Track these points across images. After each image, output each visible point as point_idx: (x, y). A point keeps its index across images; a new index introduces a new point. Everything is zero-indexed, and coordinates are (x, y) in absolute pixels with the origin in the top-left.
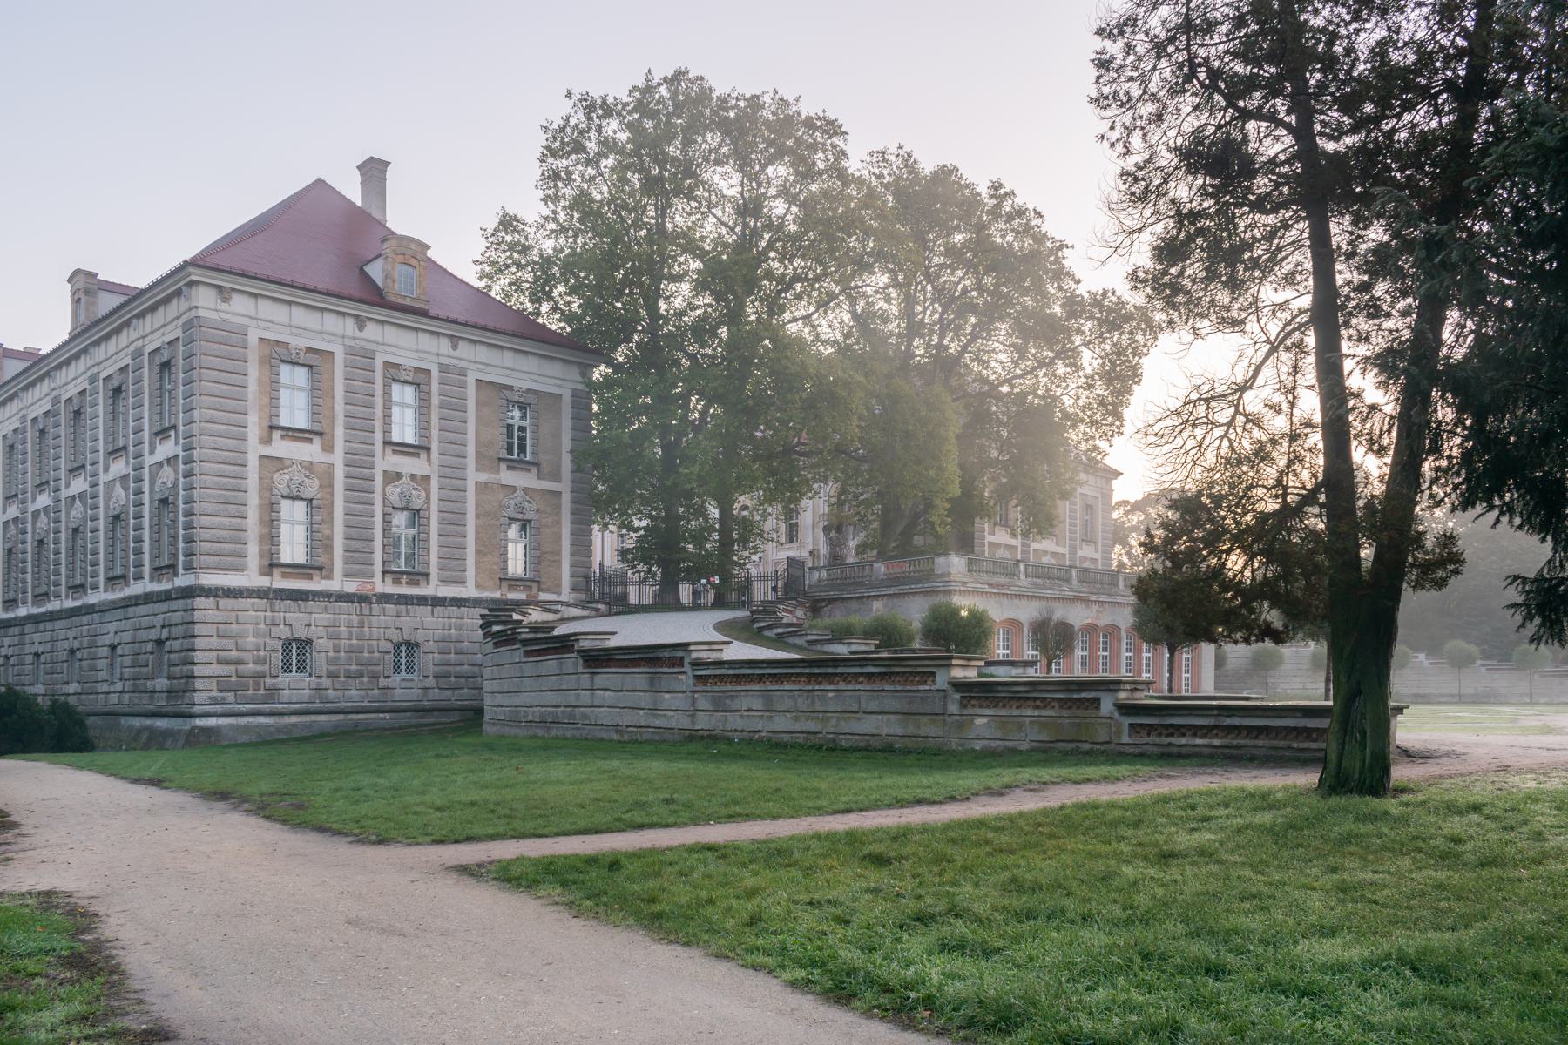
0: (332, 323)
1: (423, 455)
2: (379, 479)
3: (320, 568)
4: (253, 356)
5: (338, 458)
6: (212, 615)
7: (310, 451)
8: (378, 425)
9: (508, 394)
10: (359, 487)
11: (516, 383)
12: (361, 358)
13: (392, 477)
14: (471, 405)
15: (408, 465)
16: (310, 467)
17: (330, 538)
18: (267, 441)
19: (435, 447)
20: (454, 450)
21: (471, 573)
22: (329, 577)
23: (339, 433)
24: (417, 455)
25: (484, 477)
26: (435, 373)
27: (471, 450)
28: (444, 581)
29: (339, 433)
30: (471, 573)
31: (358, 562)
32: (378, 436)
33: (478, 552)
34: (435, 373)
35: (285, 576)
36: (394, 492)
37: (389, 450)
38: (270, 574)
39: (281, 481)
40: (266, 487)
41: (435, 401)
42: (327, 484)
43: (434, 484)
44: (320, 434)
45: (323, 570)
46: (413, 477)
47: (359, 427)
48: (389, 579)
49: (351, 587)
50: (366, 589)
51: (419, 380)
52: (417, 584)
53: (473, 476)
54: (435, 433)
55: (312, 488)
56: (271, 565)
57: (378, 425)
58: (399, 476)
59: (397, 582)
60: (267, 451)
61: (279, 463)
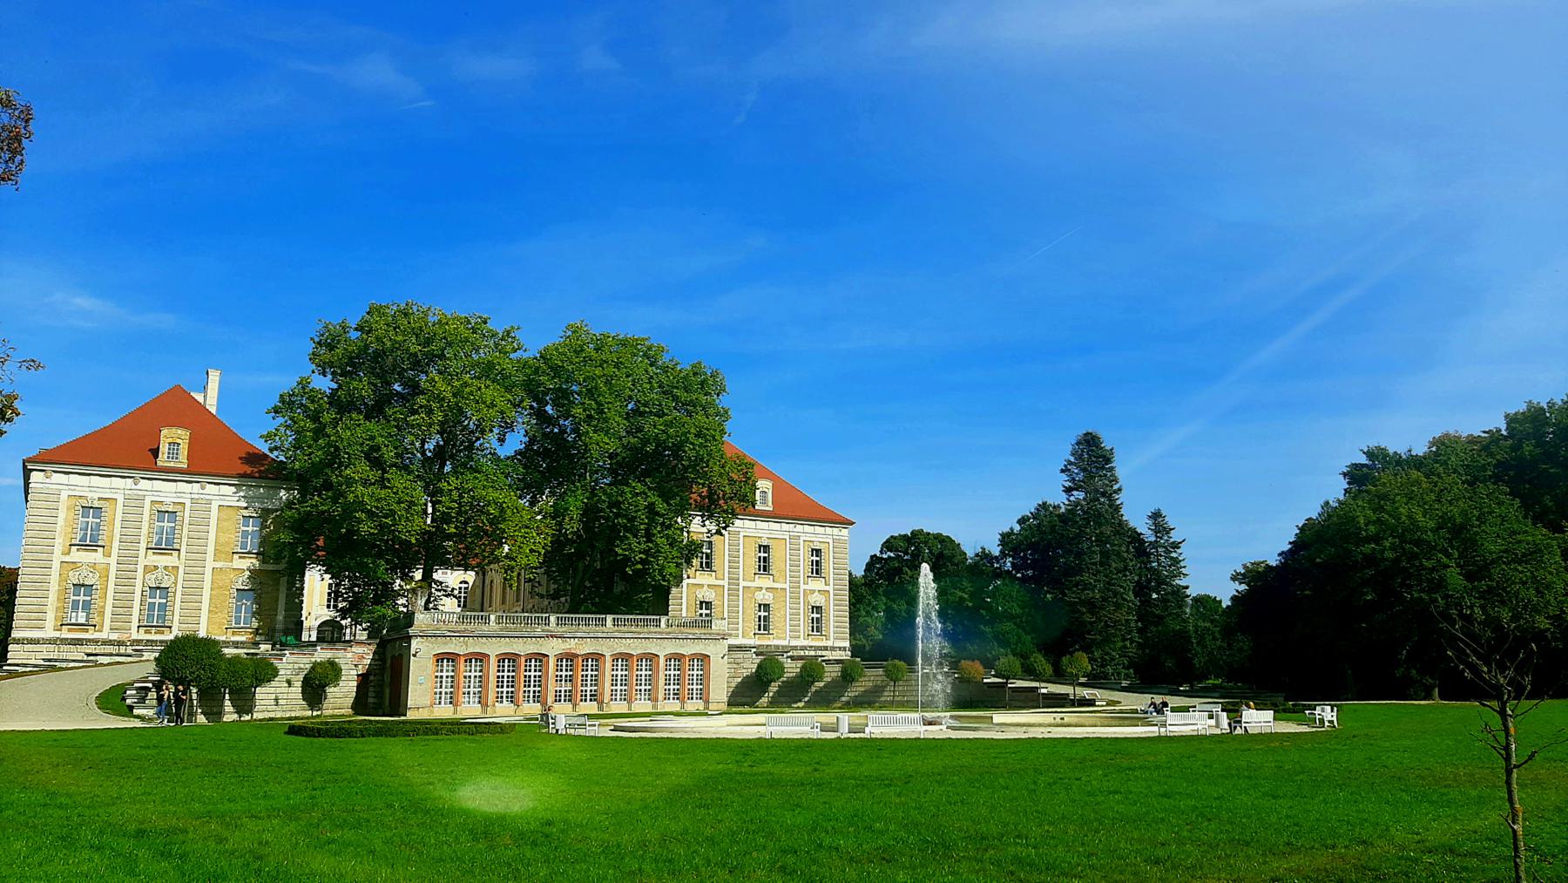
0: (117, 482)
1: (175, 554)
2: (140, 570)
4: (63, 507)
5: (113, 560)
6: (18, 655)
7: (97, 557)
10: (125, 579)
12: (135, 502)
14: (213, 522)
15: (162, 561)
23: (116, 544)
25: (219, 565)
27: (211, 549)
29: (116, 544)
32: (143, 545)
43: (181, 571)
46: (166, 568)
49: (114, 636)
50: (124, 637)
53: (210, 564)
58: (156, 567)
60: (67, 559)
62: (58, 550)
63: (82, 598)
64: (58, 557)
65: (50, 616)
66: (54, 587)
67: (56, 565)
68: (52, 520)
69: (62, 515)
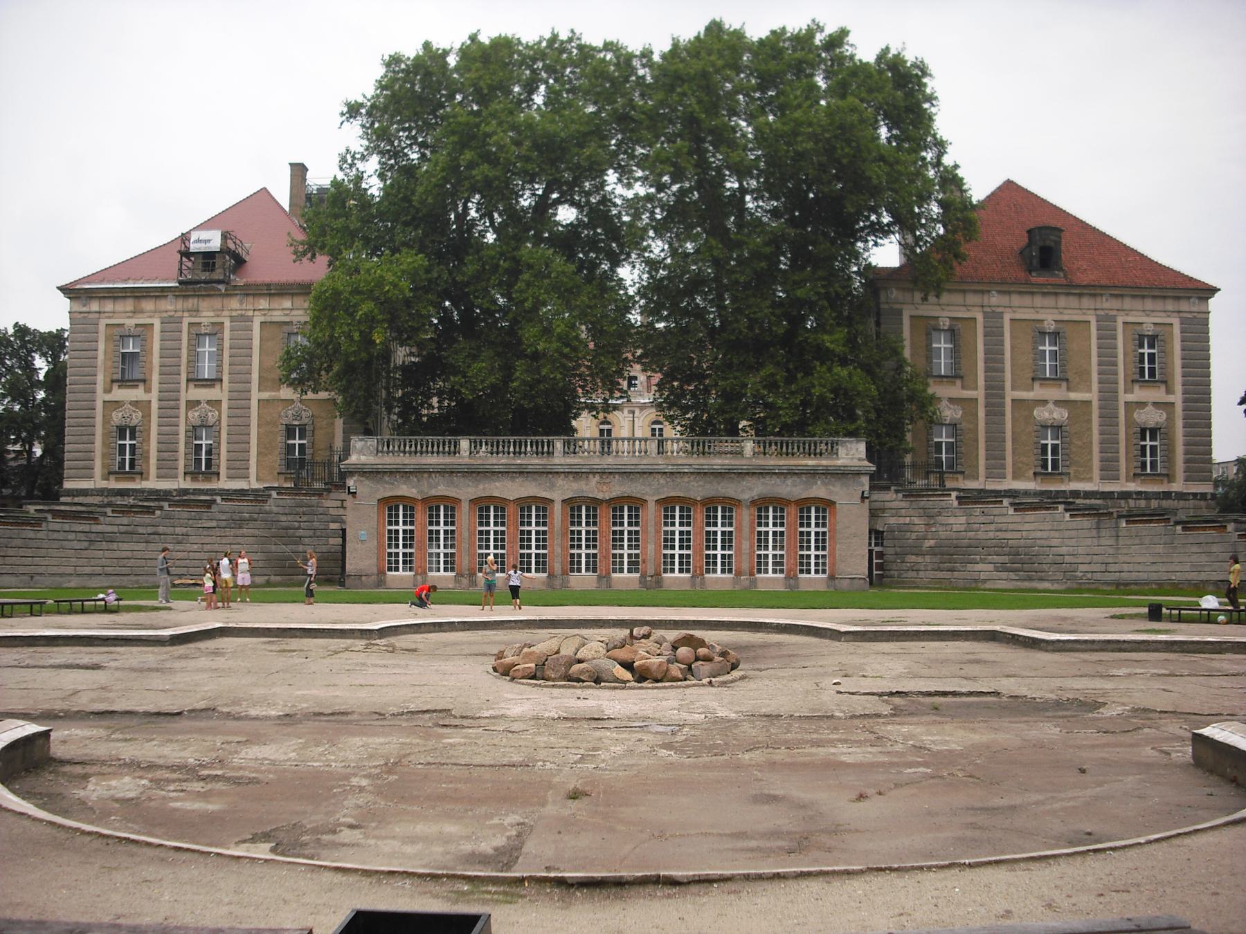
1: (218, 386)
3: (141, 474)
5: (154, 396)
7: (138, 394)
8: (183, 368)
9: (287, 329)
11: (295, 319)
13: (192, 404)
14: (256, 342)
16: (135, 403)
17: (148, 452)
18: (108, 390)
19: (226, 378)
20: (240, 378)
21: (253, 470)
22: (147, 479)
23: (155, 378)
24: (212, 386)
25: (266, 395)
26: (227, 324)
27: (255, 376)
28: (230, 477)
29: (155, 378)
30: (253, 470)
31: (166, 469)
32: (184, 377)
33: (259, 454)
34: (227, 324)
35: (117, 480)
36: (194, 415)
37: (191, 385)
38: (108, 479)
39: (117, 418)
40: (107, 419)
41: (227, 344)
42: (147, 416)
43: (225, 406)
44: (144, 381)
45: (143, 475)
46: (209, 402)
47: (169, 372)
48: (188, 478)
51: (216, 331)
52: (208, 480)
53: (256, 395)
54: (226, 368)
55: (136, 418)
56: (108, 475)
57: (183, 368)
58: (198, 402)
59: (194, 479)
60: (108, 397)
61: (117, 404)
62: (100, 388)
63: (128, 442)
64: (101, 396)
65: (98, 464)
66: (99, 430)
67: (99, 405)
68: (91, 354)
69: (101, 346)
